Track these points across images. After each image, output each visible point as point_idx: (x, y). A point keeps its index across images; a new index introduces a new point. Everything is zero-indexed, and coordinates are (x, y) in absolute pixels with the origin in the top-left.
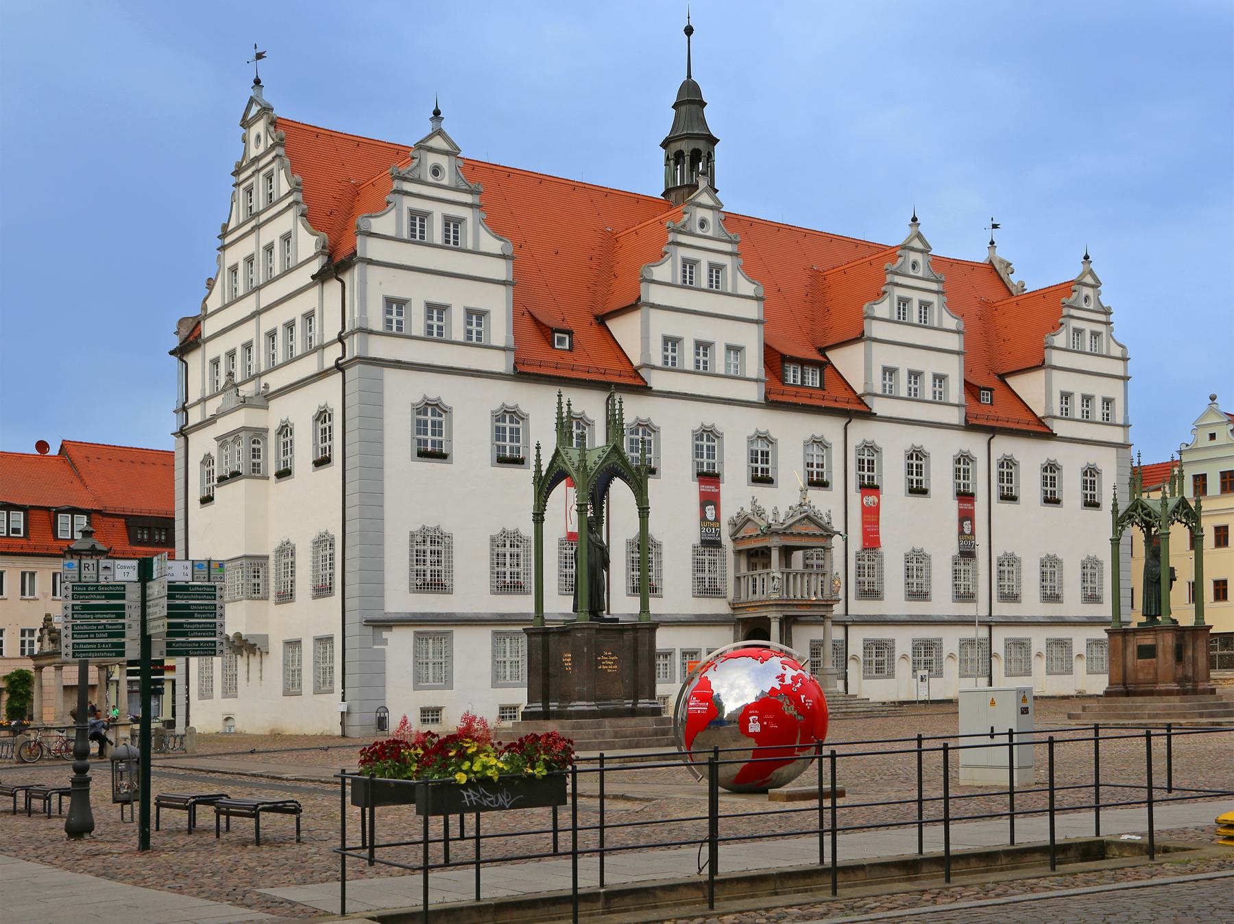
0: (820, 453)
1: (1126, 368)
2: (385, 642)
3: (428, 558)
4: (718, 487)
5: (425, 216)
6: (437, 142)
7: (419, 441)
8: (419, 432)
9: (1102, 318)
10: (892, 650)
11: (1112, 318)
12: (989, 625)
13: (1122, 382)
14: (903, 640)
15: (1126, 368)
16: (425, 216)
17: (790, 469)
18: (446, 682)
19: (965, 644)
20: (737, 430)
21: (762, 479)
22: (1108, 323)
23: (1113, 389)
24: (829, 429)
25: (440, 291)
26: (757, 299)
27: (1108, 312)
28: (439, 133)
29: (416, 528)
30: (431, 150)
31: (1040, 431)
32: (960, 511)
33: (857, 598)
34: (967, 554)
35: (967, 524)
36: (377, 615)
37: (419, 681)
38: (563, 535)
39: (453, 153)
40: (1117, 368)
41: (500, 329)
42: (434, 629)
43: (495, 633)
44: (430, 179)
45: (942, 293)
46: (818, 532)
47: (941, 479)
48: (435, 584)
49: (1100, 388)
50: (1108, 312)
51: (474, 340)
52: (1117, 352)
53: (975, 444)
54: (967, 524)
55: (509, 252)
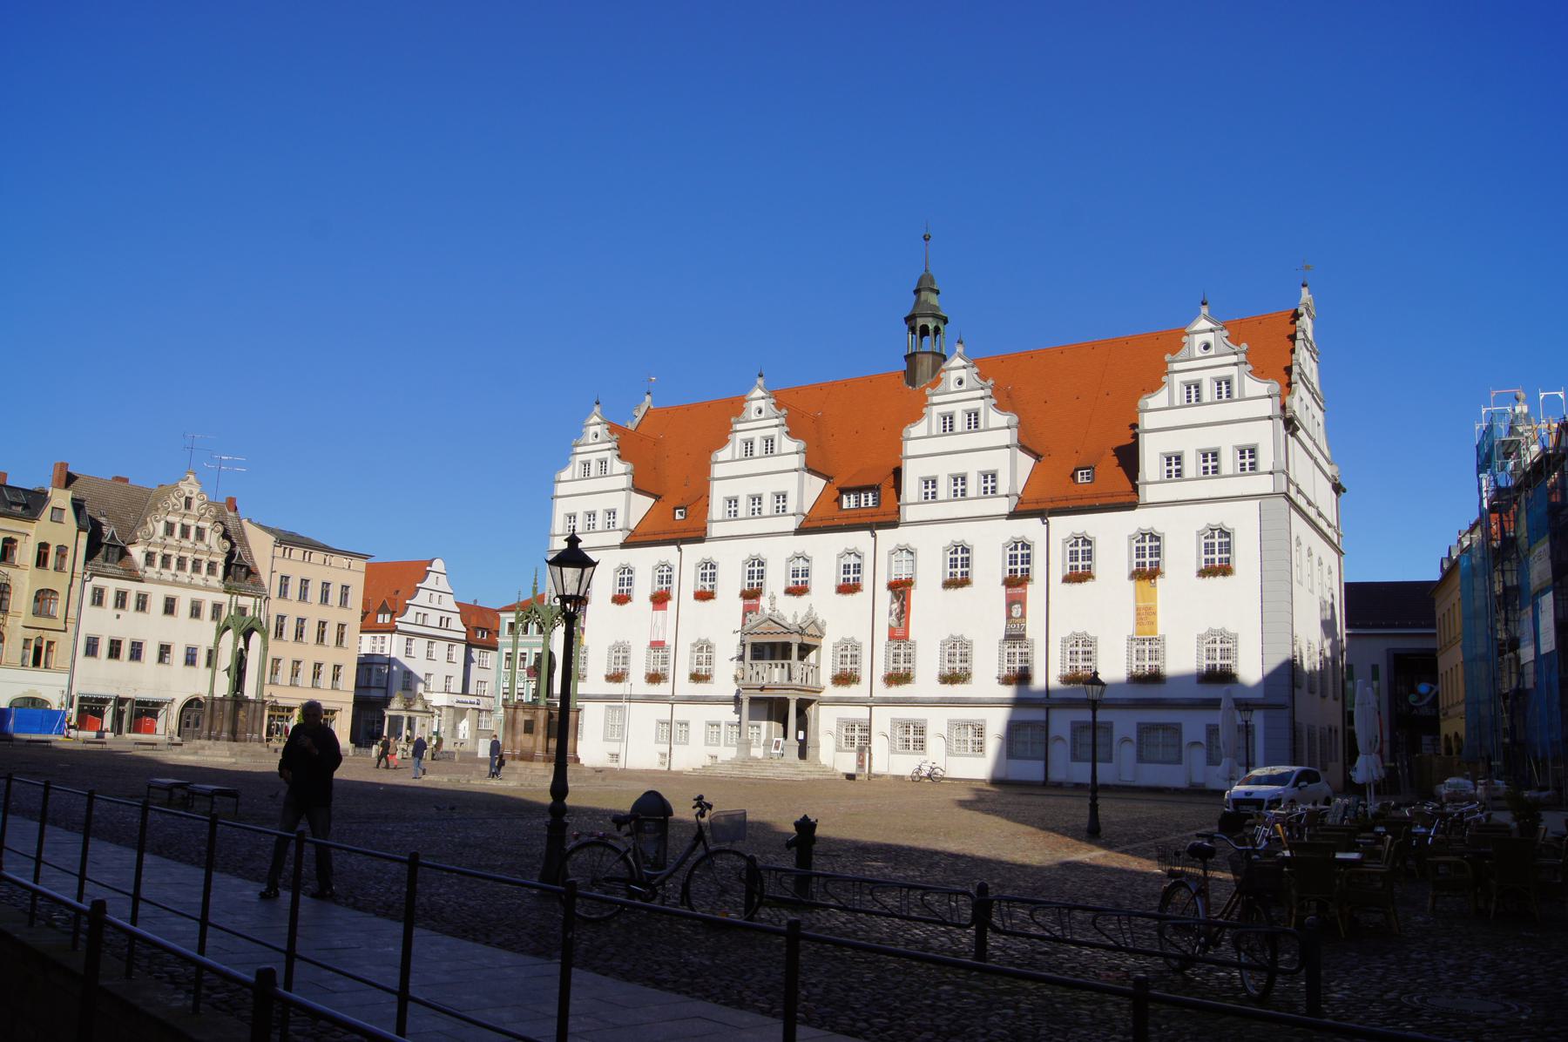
17: (824, 578)
20: (779, 555)
21: (798, 591)
32: (1007, 596)
47: (989, 569)
48: (616, 678)
53: (1031, 528)
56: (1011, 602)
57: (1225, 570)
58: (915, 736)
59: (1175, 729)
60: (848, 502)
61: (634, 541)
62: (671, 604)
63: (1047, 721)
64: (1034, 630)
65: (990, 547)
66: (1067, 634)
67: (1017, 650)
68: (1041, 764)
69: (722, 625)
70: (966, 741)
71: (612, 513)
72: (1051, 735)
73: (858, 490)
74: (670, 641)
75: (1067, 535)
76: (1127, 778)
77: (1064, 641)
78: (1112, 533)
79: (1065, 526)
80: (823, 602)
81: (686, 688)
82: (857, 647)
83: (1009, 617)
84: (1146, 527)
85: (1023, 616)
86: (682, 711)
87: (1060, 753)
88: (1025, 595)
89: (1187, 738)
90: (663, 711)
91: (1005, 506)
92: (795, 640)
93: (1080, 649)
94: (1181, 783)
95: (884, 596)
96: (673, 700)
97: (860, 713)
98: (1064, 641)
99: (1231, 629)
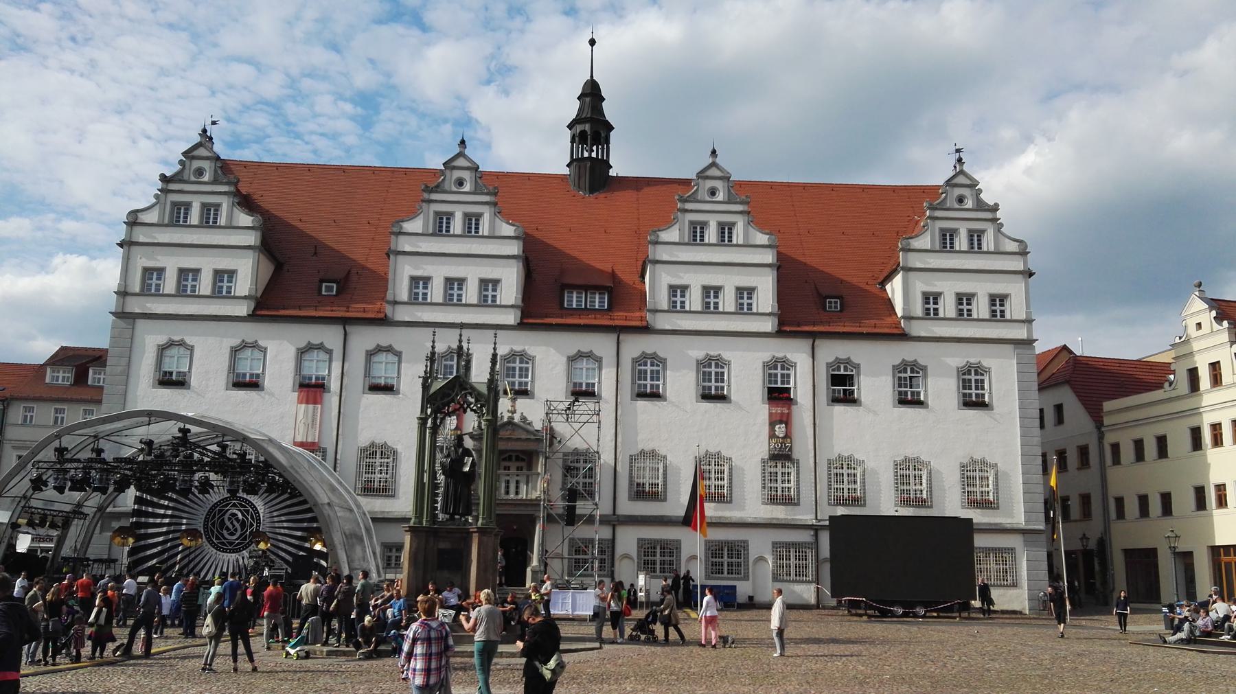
0: (591, 366)
1: (1025, 263)
3: (713, 475)
4: (789, 408)
8: (964, 388)
9: (989, 215)
10: (679, 549)
19: (776, 545)
22: (995, 220)
24: (601, 344)
27: (995, 208)
30: (708, 178)
32: (771, 414)
33: (630, 499)
34: (782, 455)
39: (726, 178)
41: (766, 299)
44: (957, 206)
45: (749, 213)
50: (995, 208)
51: (743, 309)
52: (1013, 247)
53: (797, 353)
62: (332, 400)
69: (394, 422)
75: (831, 359)
79: (831, 350)
83: (772, 435)
85: (787, 436)
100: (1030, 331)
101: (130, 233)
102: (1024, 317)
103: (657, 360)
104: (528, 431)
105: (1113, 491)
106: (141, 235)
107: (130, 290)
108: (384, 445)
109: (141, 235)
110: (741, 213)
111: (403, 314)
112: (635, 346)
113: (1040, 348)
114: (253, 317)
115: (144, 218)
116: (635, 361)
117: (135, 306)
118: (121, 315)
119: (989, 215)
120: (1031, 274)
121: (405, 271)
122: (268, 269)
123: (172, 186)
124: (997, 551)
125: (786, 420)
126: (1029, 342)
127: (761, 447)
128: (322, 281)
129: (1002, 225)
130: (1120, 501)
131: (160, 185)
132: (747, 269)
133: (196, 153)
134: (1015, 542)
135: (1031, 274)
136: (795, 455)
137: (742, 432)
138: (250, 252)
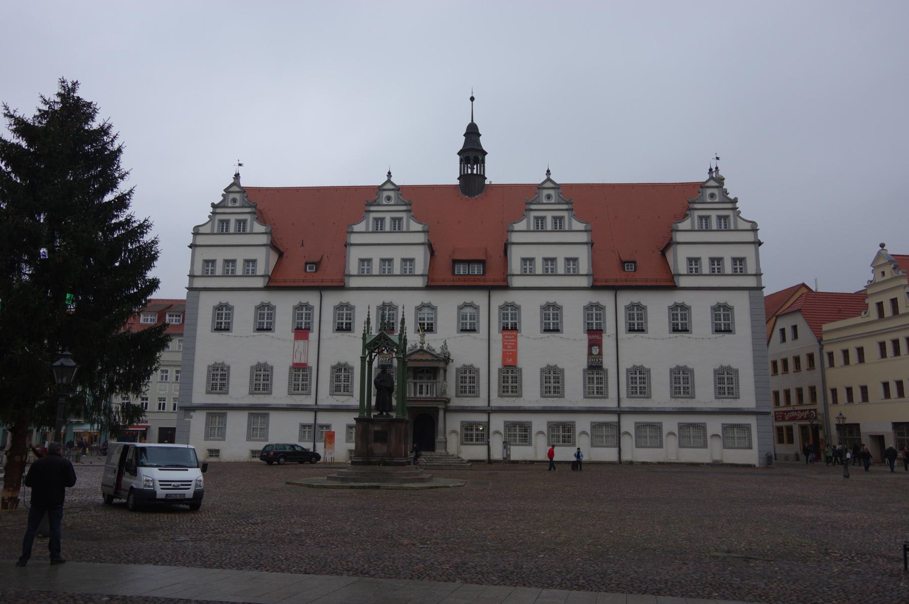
2: (191, 417)
5: (543, 218)
6: (235, 188)
7: (716, 324)
9: (730, 206)
11: (738, 205)
12: (619, 412)
13: (752, 247)
14: (539, 423)
15: (756, 236)
16: (543, 218)
18: (222, 437)
20: (407, 305)
22: (734, 209)
23: (747, 252)
24: (479, 298)
25: (230, 254)
26: (586, 231)
27: (735, 201)
28: (549, 180)
29: (335, 363)
31: (669, 285)
32: (590, 340)
34: (595, 367)
35: (595, 351)
36: (187, 404)
37: (208, 436)
38: (291, 365)
40: (749, 237)
42: (217, 413)
43: (250, 414)
45: (572, 210)
46: (430, 358)
49: (727, 254)
50: (735, 201)
52: (748, 226)
53: (605, 299)
54: (595, 351)
55: (589, 228)
56: (590, 346)
57: (728, 331)
58: (522, 433)
59: (702, 427)
60: (461, 270)
61: (273, 284)
62: (313, 336)
63: (619, 422)
64: (608, 362)
65: (573, 308)
66: (630, 366)
67: (595, 376)
68: (616, 449)
70: (558, 436)
71: (250, 262)
72: (622, 430)
73: (469, 262)
74: (312, 363)
75: (628, 303)
76: (672, 458)
77: (628, 370)
78: (657, 306)
80: (446, 338)
81: (326, 399)
82: (477, 371)
83: (590, 353)
84: (679, 301)
85: (600, 353)
86: (323, 418)
87: (627, 443)
88: (601, 340)
89: (710, 433)
90: (308, 418)
91: (584, 282)
92: (442, 365)
93: (638, 376)
94: (707, 459)
95: (497, 336)
96: (316, 410)
97: (483, 418)
98: (628, 370)
99: (734, 366)
100: (759, 281)
101: (194, 239)
102: (754, 272)
103: (515, 307)
104: (432, 355)
105: (830, 385)
106: (201, 240)
107: (196, 274)
108: (346, 364)
109: (201, 240)
110: (567, 210)
111: (353, 282)
112: (500, 299)
113: (766, 292)
114: (267, 288)
115: (201, 230)
116: (502, 308)
117: (199, 283)
118: (190, 289)
119: (730, 206)
120: (760, 244)
121: (355, 255)
122: (274, 257)
123: (218, 210)
124: (739, 426)
125: (599, 344)
126: (760, 288)
127: (584, 363)
128: (306, 264)
129: (740, 212)
130: (834, 391)
131: (211, 210)
132: (573, 244)
133: (231, 189)
134: (752, 421)
135: (760, 244)
136: (605, 366)
137: (570, 352)
138: (264, 249)
